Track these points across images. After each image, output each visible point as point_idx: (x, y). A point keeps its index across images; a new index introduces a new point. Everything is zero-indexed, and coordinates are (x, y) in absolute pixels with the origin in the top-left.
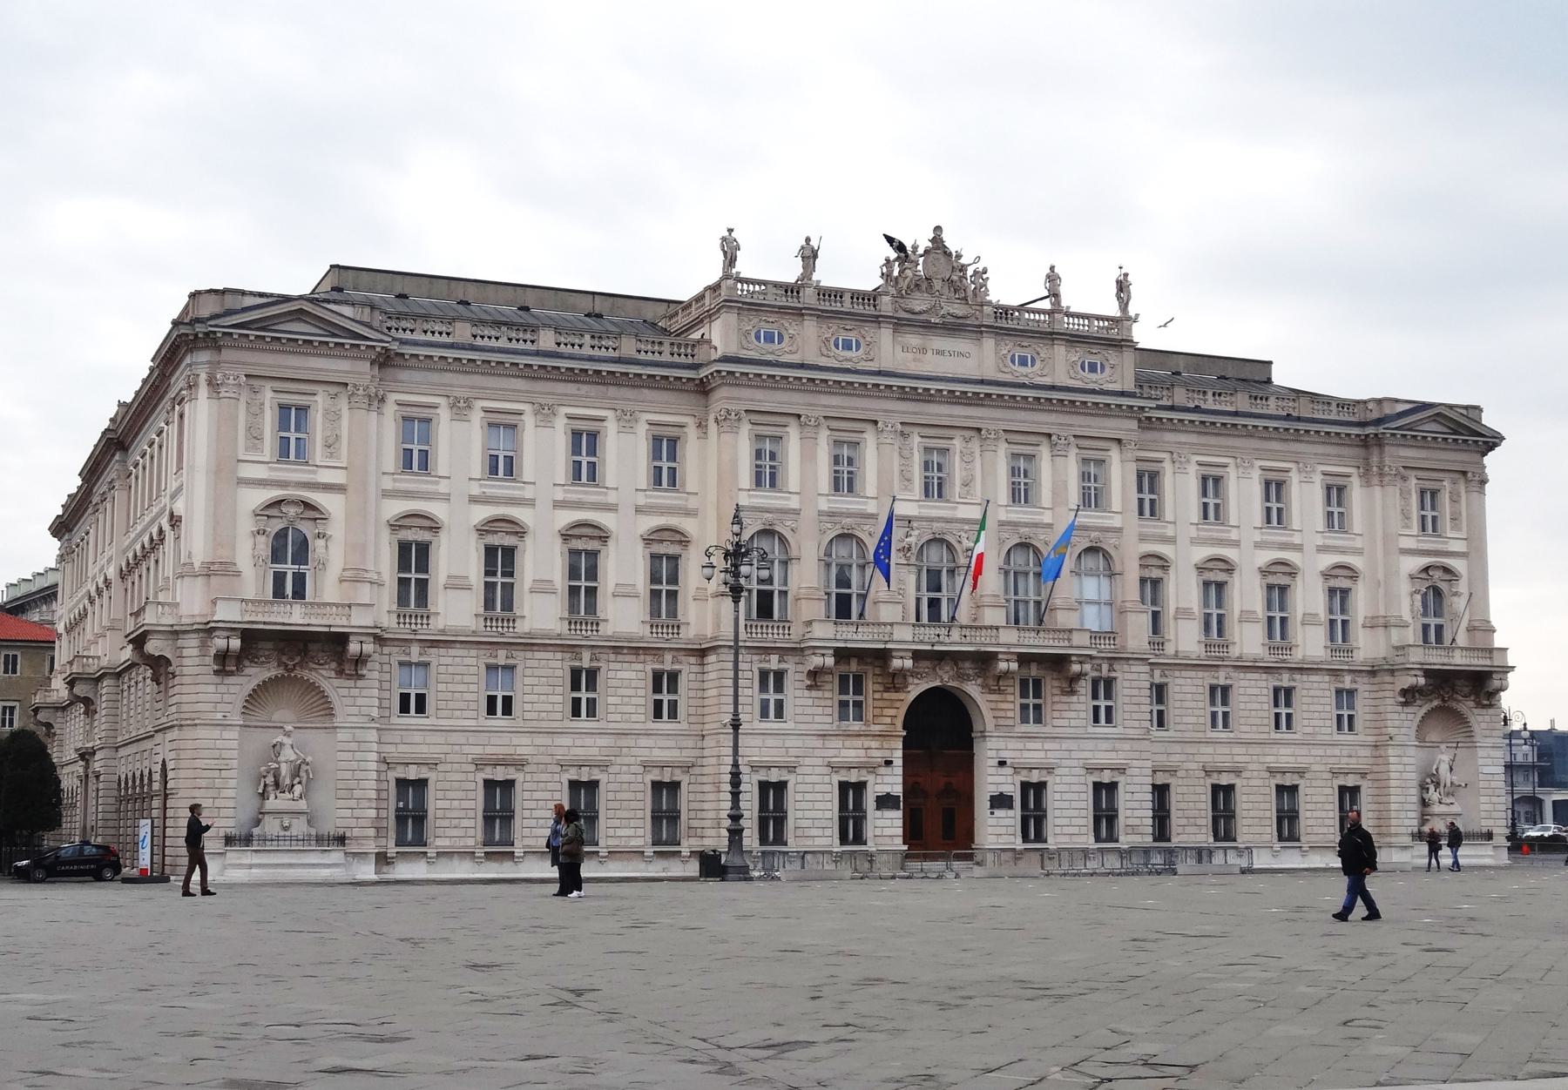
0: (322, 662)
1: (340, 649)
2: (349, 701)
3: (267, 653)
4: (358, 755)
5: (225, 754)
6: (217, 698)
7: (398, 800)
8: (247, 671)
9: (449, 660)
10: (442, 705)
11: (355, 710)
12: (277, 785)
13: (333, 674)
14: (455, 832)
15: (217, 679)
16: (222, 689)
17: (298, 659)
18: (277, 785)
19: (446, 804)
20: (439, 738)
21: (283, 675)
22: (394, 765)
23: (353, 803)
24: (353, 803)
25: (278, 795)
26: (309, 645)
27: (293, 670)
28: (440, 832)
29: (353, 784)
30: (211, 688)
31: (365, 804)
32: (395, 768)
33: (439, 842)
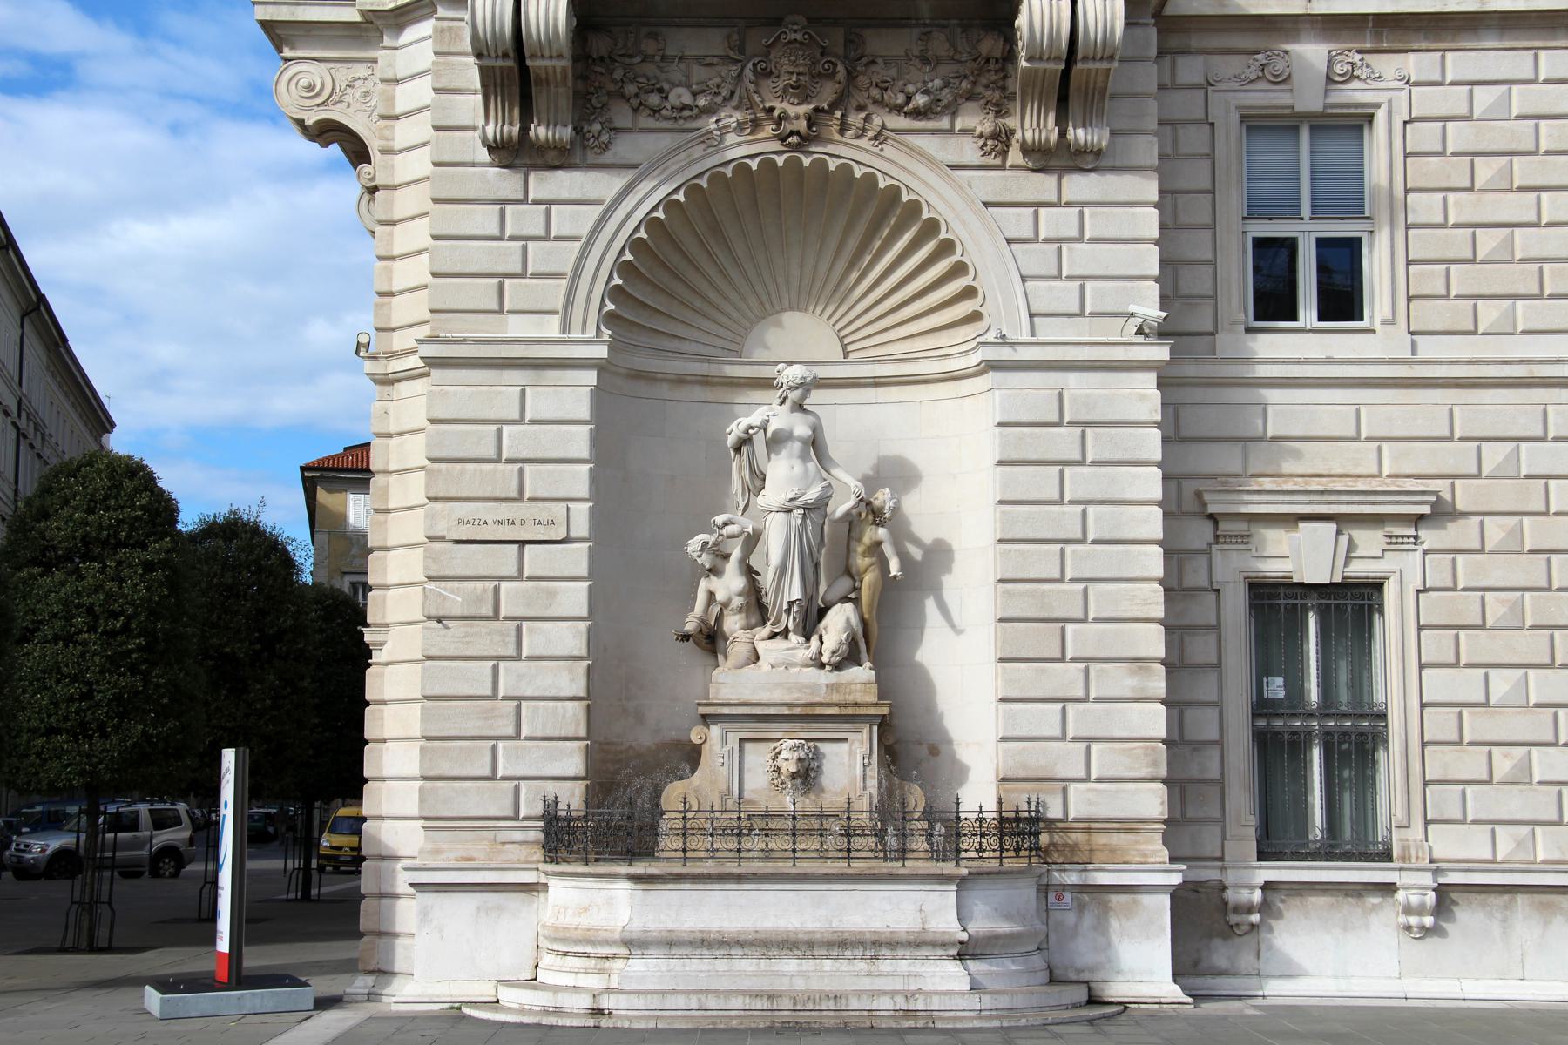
0: (920, 100)
1: (990, 45)
2: (1037, 258)
3: (699, 73)
4: (1079, 481)
5: (537, 480)
6: (506, 256)
7: (1263, 669)
8: (624, 148)
9: (1451, 100)
10: (1429, 279)
11: (1063, 296)
12: (757, 605)
13: (969, 151)
14: (1514, 803)
15: (504, 182)
16: (525, 219)
17: (826, 93)
18: (757, 605)
19: (1466, 685)
20: (1425, 411)
21: (767, 164)
22: (1241, 527)
23: (1066, 678)
24: (1066, 678)
25: (762, 647)
26: (868, 33)
27: (806, 141)
28: (1444, 801)
29: (1065, 599)
30: (483, 219)
31: (1119, 680)
32: (1244, 538)
33: (1445, 843)
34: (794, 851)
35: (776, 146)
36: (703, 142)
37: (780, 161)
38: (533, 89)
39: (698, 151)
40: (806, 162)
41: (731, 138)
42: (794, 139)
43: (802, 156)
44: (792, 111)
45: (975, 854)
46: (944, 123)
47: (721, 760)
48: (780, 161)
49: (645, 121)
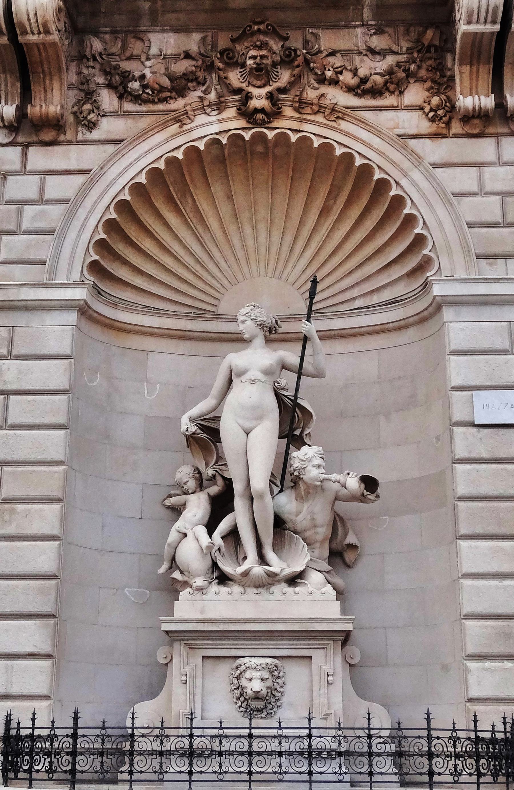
34: (250, 773)
35: (242, 123)
36: (180, 121)
37: (247, 135)
38: (31, 77)
39: (174, 128)
40: (270, 135)
41: (201, 119)
42: (260, 116)
43: (264, 130)
44: (255, 92)
45: (450, 779)
46: (390, 100)
47: (184, 678)
48: (247, 135)
49: (129, 106)
